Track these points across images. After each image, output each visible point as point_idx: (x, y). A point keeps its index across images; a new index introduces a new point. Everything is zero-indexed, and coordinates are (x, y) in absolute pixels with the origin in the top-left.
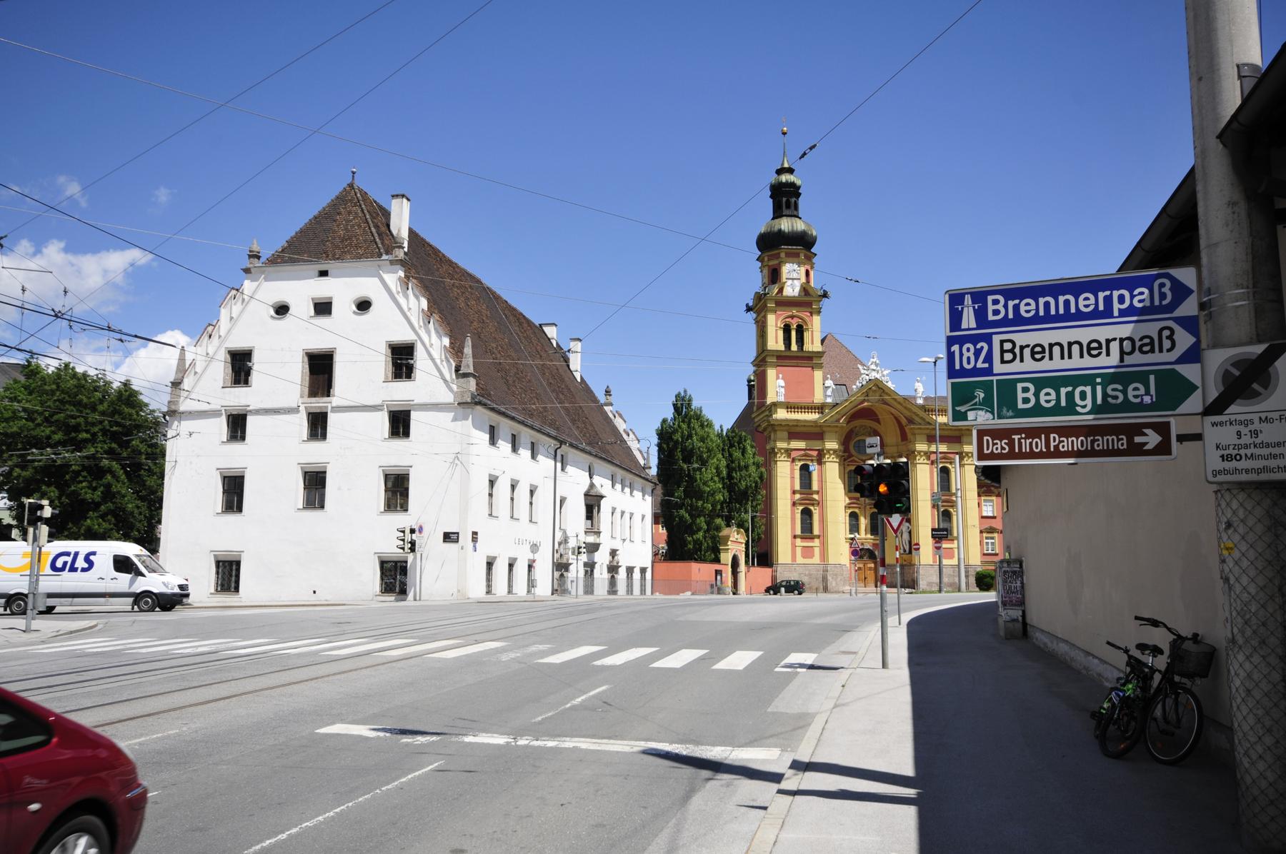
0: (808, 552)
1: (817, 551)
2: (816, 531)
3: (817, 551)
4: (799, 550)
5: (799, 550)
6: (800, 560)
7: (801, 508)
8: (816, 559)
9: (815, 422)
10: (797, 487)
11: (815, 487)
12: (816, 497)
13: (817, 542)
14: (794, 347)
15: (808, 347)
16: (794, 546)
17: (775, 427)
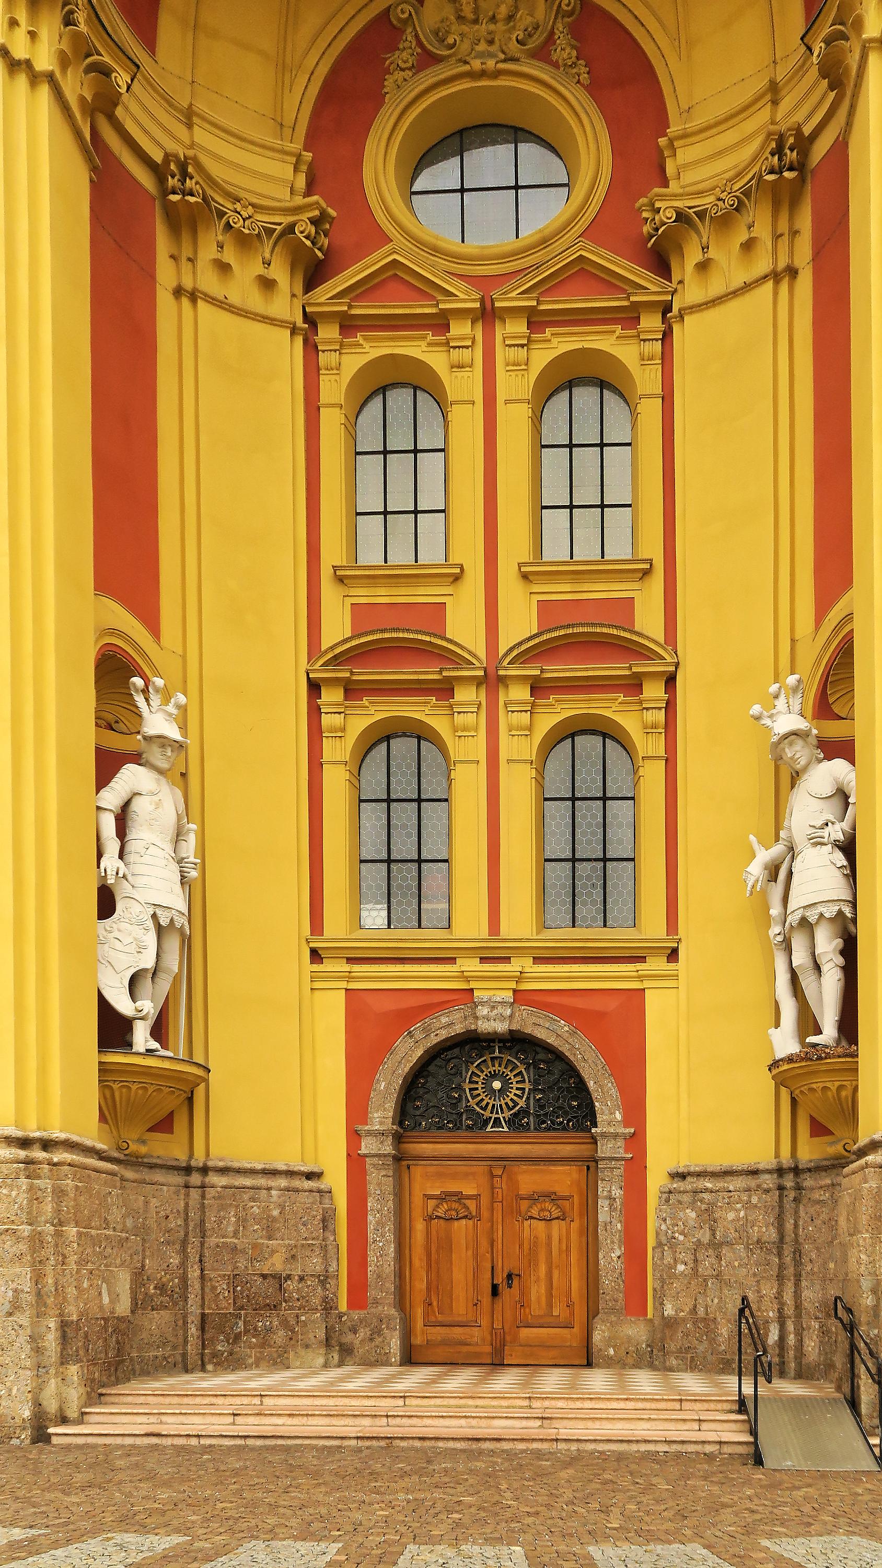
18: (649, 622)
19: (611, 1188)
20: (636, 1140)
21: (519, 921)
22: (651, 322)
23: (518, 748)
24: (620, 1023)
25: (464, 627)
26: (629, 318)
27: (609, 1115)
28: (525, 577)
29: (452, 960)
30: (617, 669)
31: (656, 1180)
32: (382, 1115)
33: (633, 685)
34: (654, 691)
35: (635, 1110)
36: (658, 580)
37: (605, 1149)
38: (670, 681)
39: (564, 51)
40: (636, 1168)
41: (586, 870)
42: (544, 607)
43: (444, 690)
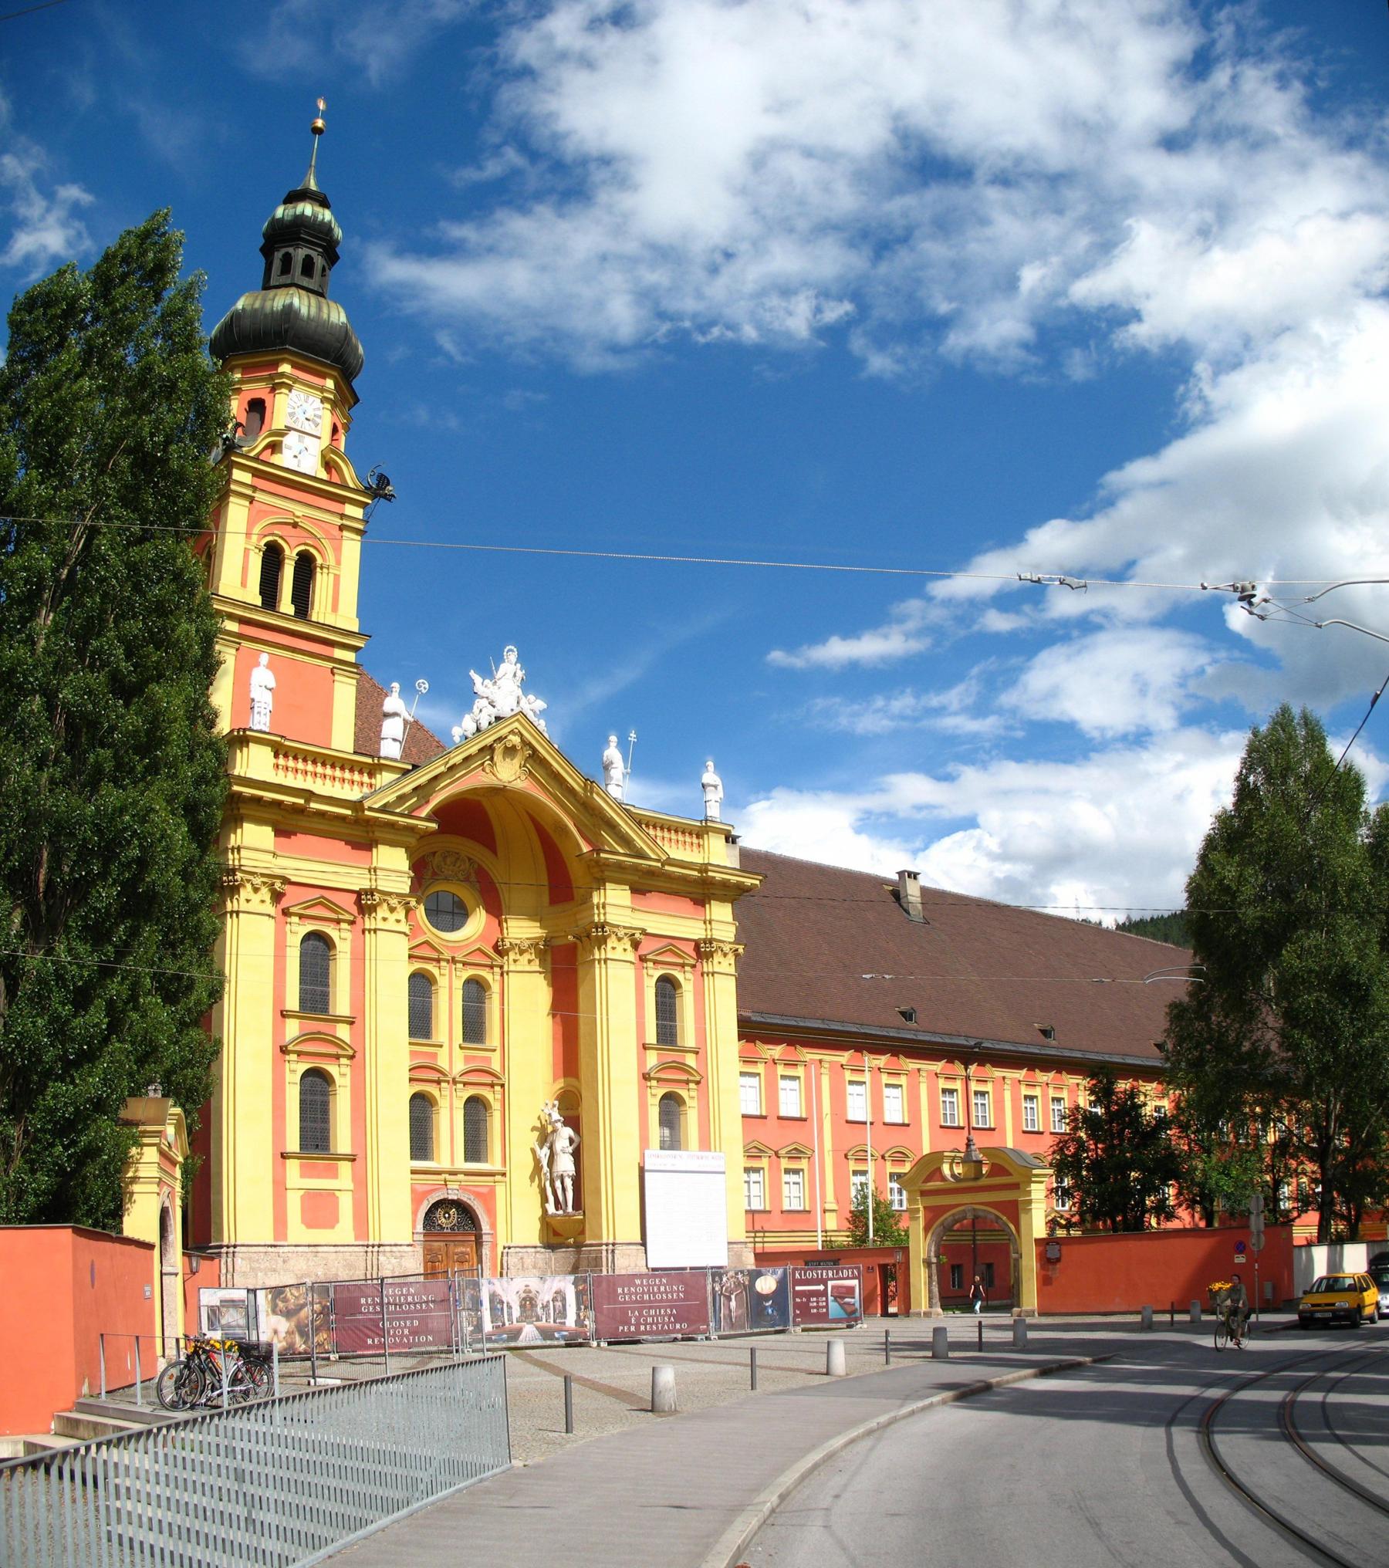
0: (321, 1209)
1: (346, 1204)
2: (342, 1140)
3: (346, 1204)
4: (294, 1202)
5: (294, 1202)
6: (297, 1231)
7: (303, 1067)
8: (344, 1231)
9: (357, 806)
10: (293, 1002)
11: (341, 1005)
12: (343, 1032)
13: (344, 1177)
14: (286, 606)
15: (320, 611)
16: (280, 1188)
17: (242, 807)
18: (496, 1066)
19: (486, 1251)
20: (494, 1235)
21: (461, 1164)
22: (497, 970)
23: (460, 1105)
24: (489, 1198)
25: (443, 1062)
26: (492, 967)
27: (485, 1228)
28: (461, 1048)
29: (439, 1173)
30: (488, 1079)
31: (500, 1249)
32: (420, 1228)
33: (492, 1085)
34: (498, 1088)
35: (493, 1226)
36: (498, 1053)
37: (485, 1238)
38: (503, 1086)
39: (473, 878)
40: (494, 1245)
41: (475, 1147)
42: (467, 1059)
43: (438, 1082)
